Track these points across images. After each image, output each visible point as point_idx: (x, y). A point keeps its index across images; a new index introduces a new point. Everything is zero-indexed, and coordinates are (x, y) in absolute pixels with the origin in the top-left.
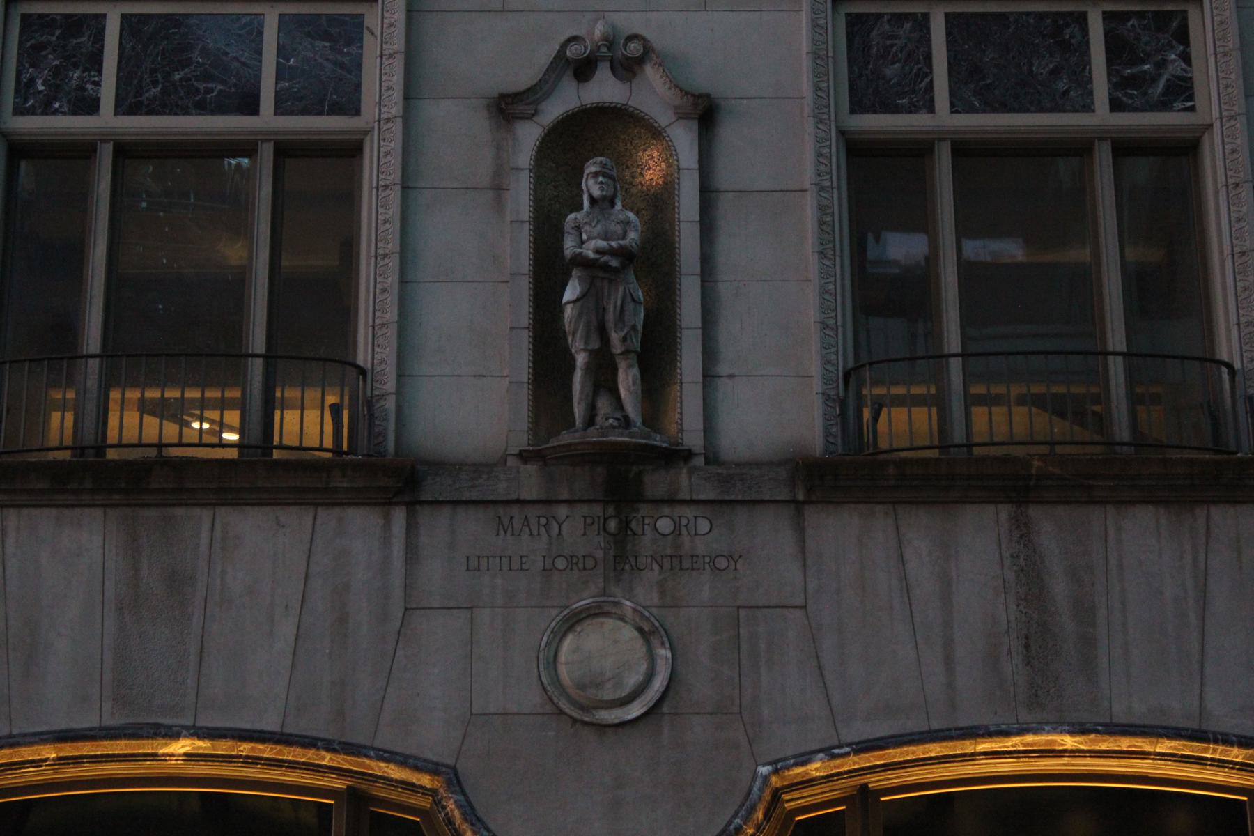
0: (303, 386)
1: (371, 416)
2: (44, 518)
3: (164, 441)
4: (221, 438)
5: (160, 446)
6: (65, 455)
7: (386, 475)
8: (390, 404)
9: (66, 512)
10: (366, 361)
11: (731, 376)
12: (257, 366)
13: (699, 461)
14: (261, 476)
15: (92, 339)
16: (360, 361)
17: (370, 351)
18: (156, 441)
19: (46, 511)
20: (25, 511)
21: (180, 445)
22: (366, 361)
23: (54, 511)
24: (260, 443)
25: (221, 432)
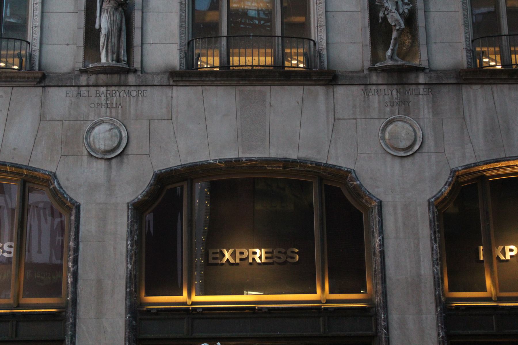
0: (253, 47)
1: (320, 56)
2: (505, 88)
3: (254, 64)
4: (291, 63)
5: (252, 66)
6: (271, 68)
7: (323, 75)
8: (325, 52)
9: (512, 86)
10: (315, 37)
11: (435, 43)
12: (224, 41)
13: (427, 71)
14: (278, 75)
15: (505, 29)
16: (313, 38)
17: (316, 35)
18: (251, 64)
19: (505, 85)
20: (499, 86)
21: (246, 66)
22: (315, 37)
23: (507, 86)
24: (225, 66)
25: (291, 61)
